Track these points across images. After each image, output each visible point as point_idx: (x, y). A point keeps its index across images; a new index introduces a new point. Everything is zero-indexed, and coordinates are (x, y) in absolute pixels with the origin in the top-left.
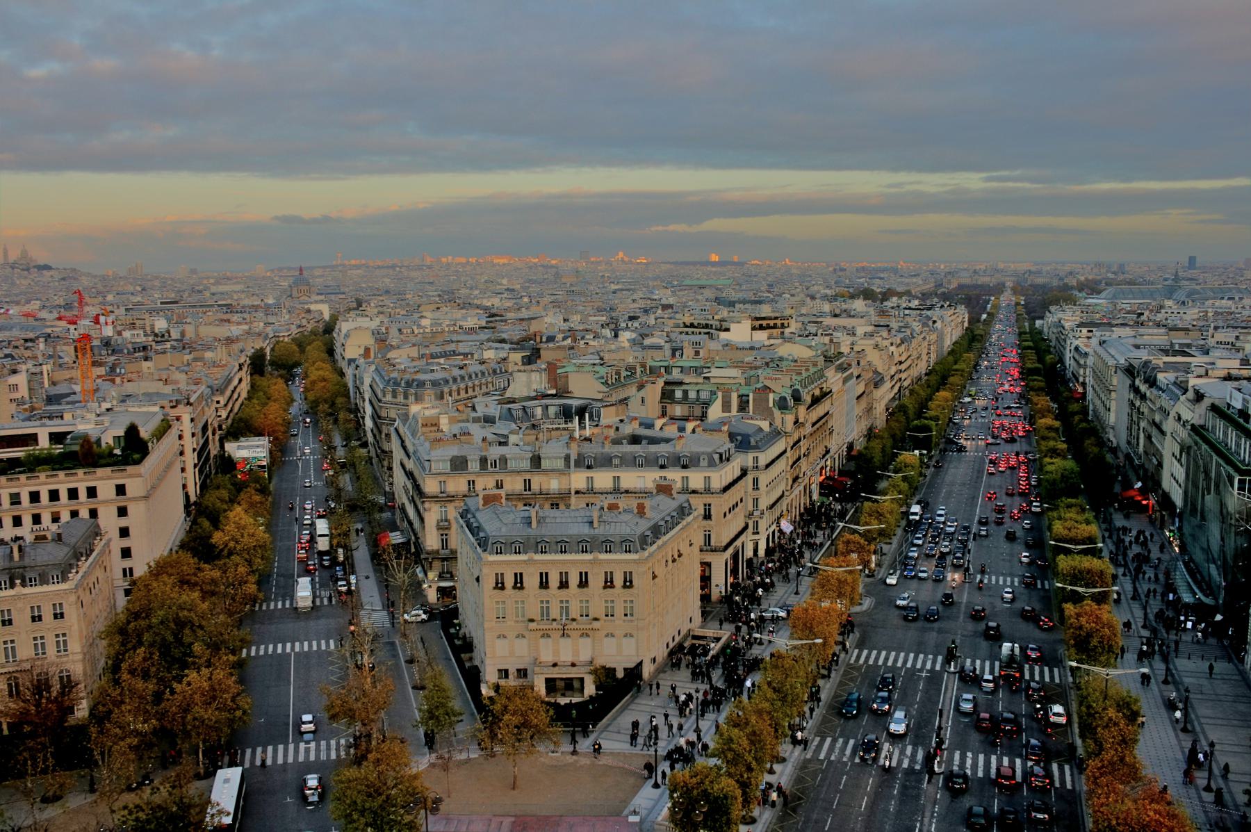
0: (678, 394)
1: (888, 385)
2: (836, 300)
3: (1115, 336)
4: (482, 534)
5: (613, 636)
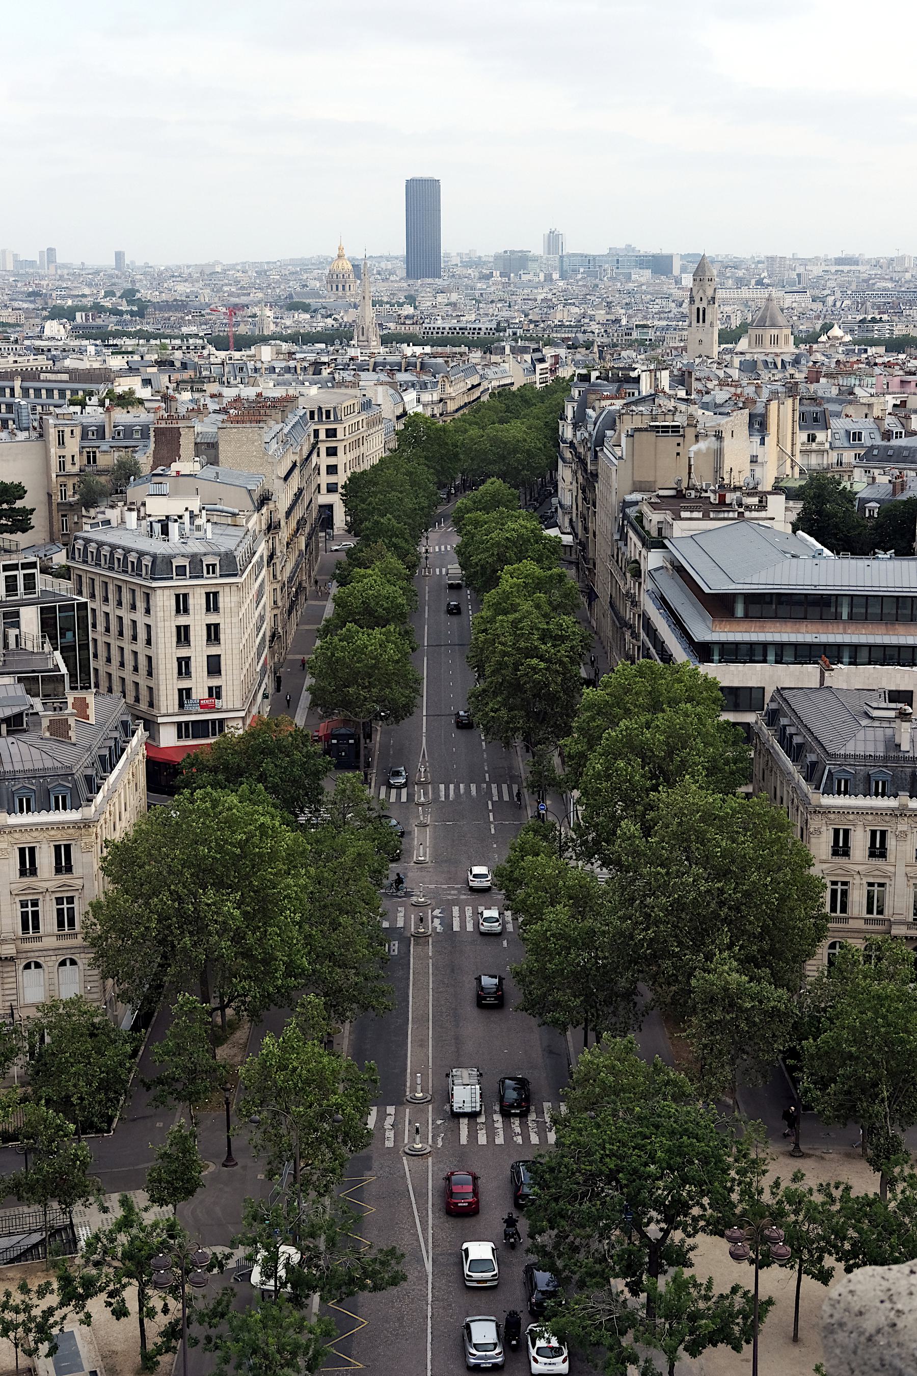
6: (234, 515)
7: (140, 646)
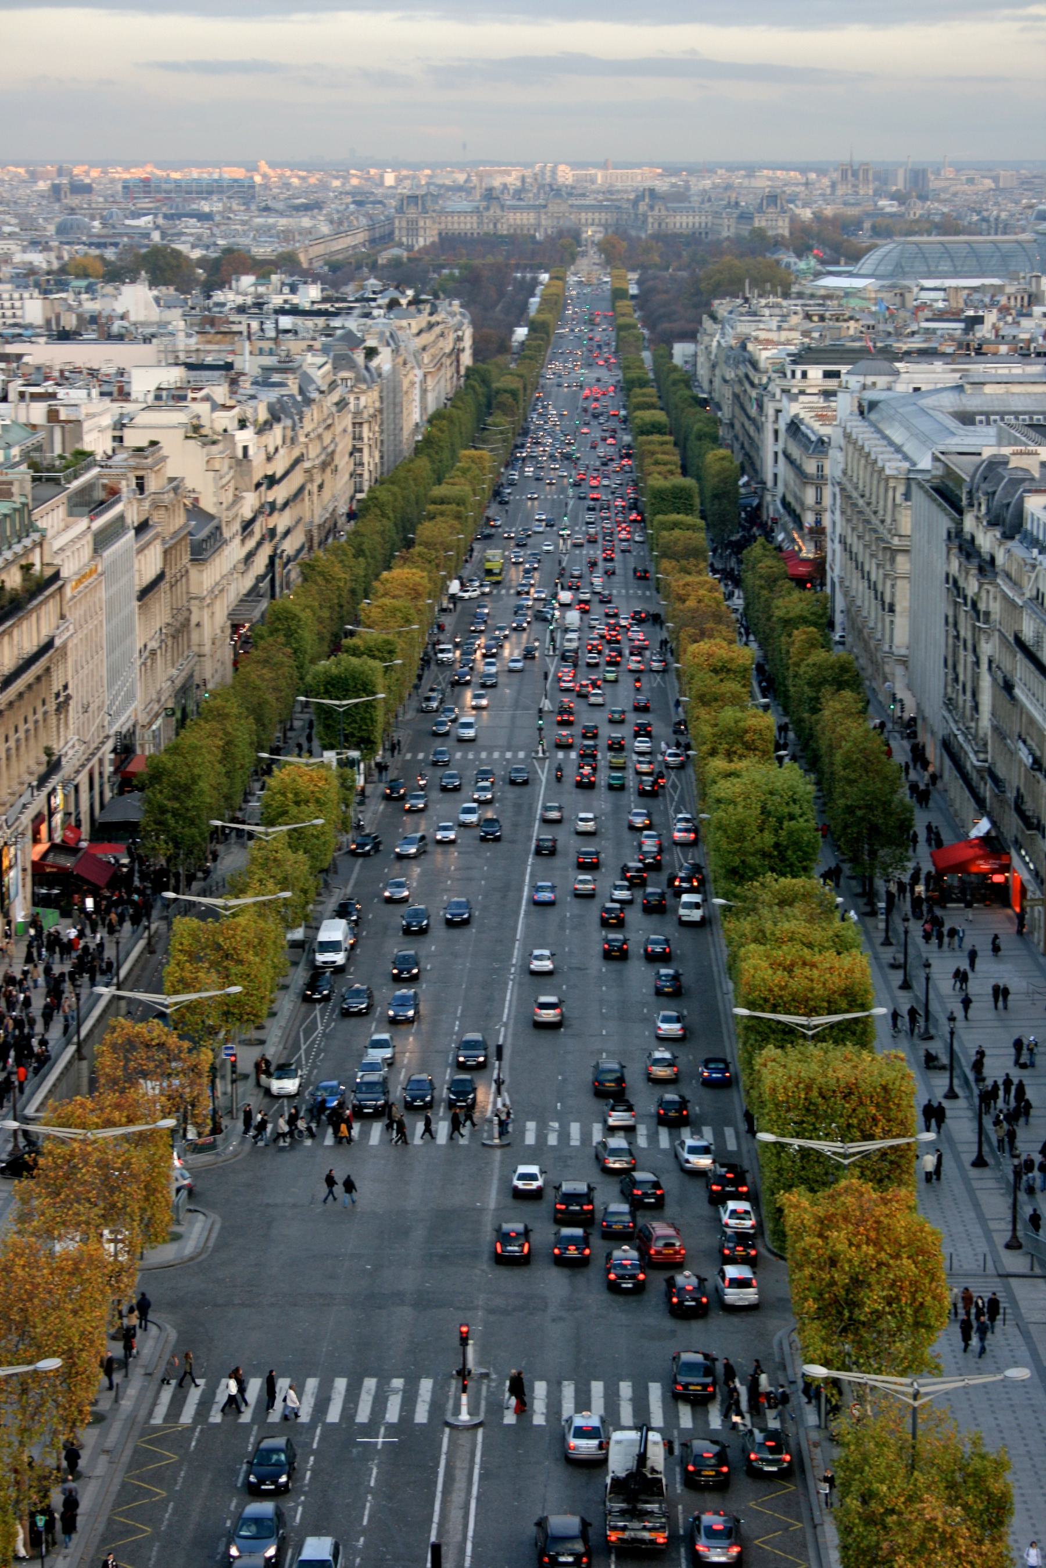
1: (234, 551)
2: (63, 287)
3: (902, 387)
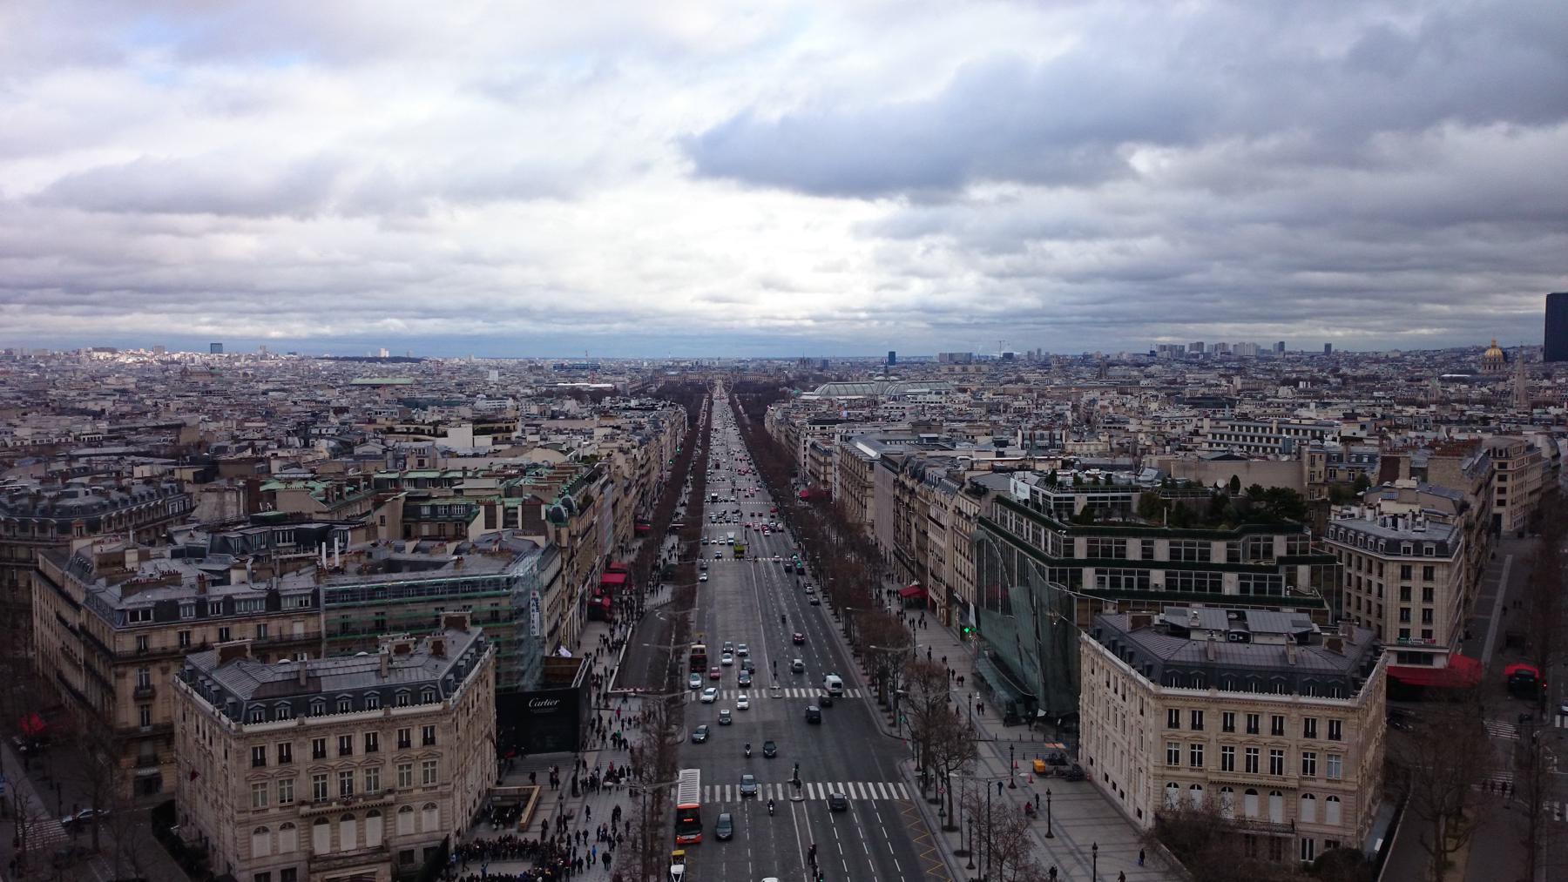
0: (426, 511)
1: (634, 491)
4: (230, 700)
5: (410, 809)
6: (1445, 516)
7: (1373, 597)
